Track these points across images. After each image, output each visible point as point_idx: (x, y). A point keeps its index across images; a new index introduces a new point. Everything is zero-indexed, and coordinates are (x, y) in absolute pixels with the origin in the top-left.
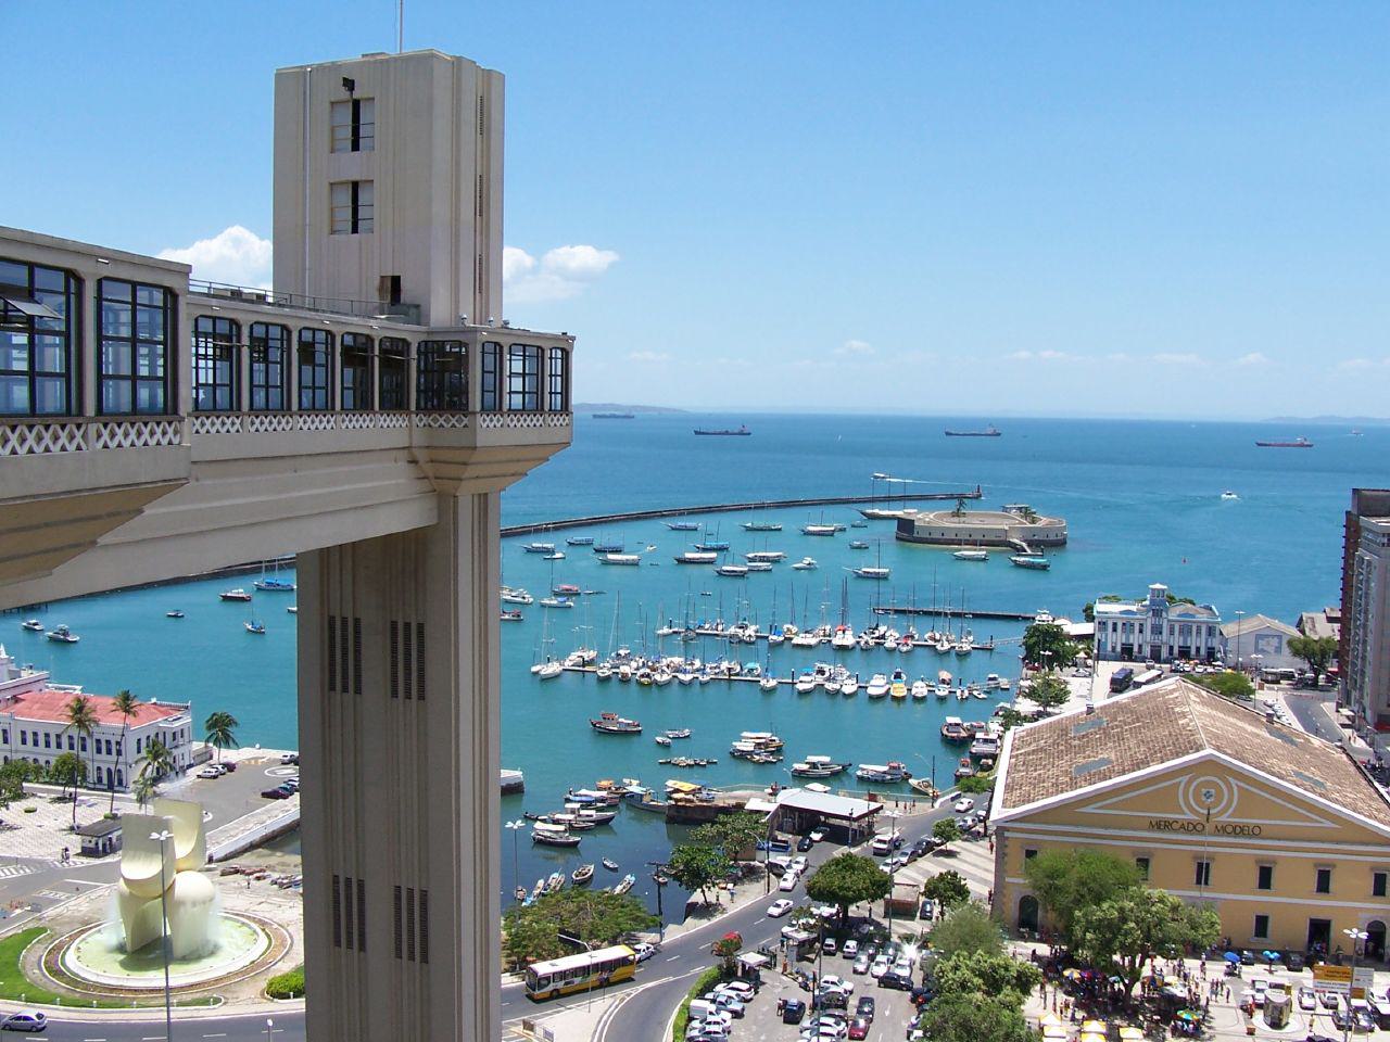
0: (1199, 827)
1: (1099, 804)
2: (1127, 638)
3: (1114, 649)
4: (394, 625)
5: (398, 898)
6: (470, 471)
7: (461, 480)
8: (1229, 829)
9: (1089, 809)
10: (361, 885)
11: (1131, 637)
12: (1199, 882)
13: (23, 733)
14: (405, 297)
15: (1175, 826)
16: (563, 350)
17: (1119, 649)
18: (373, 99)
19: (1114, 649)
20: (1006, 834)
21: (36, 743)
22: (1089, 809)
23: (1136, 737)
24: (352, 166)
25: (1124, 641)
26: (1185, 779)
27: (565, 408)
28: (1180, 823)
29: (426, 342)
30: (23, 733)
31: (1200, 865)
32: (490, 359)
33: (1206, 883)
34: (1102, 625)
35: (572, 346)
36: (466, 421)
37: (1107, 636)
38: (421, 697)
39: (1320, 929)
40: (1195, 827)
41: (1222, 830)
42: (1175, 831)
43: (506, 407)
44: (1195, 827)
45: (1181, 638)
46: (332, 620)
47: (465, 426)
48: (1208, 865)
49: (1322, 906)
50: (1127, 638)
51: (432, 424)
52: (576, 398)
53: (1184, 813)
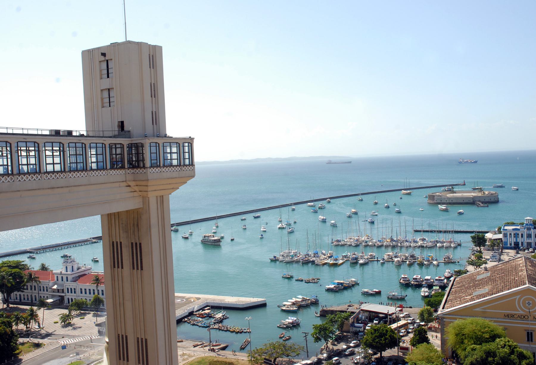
0: (526, 317)
1: (479, 308)
2: (516, 240)
3: (511, 244)
4: (132, 243)
5: (138, 342)
6: (150, 189)
7: (147, 191)
9: (478, 309)
10: (126, 337)
11: (518, 239)
12: (528, 340)
13: (81, 289)
14: (126, 128)
15: (515, 316)
16: (189, 143)
17: (513, 245)
18: (112, 59)
19: (511, 244)
20: (444, 320)
21: (86, 293)
22: (478, 309)
23: (501, 280)
24: (106, 83)
25: (515, 241)
26: (518, 297)
27: (192, 164)
28: (517, 316)
29: (132, 144)
30: (81, 289)
31: (528, 333)
32: (153, 150)
33: (532, 341)
34: (505, 235)
35: (193, 142)
36: (145, 171)
37: (507, 239)
38: (142, 269)
40: (524, 317)
42: (516, 319)
43: (89, 168)
44: (524, 317)
45: (515, 239)
46: (113, 242)
47: (145, 173)
48: (531, 333)
50: (516, 240)
51: (135, 172)
52: (196, 159)
53: (519, 311)
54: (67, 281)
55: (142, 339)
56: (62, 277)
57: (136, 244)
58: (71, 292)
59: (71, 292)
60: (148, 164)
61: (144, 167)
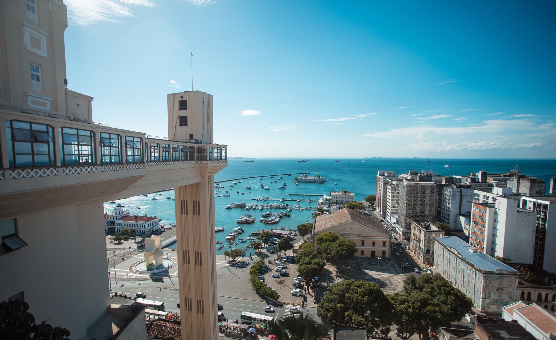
0: (350, 234)
4: (194, 201)
5: (196, 254)
6: (207, 172)
7: (205, 173)
8: (356, 235)
13: (125, 224)
17: (336, 202)
24: (183, 113)
26: (347, 225)
27: (226, 159)
29: (198, 147)
30: (125, 224)
32: (211, 150)
34: (332, 197)
36: (206, 162)
38: (199, 214)
39: (373, 253)
41: (354, 235)
49: (373, 248)
52: (228, 156)
54: (116, 219)
55: (198, 252)
56: (114, 218)
57: (196, 201)
58: (119, 226)
59: (119, 226)
60: (208, 159)
61: (206, 160)
